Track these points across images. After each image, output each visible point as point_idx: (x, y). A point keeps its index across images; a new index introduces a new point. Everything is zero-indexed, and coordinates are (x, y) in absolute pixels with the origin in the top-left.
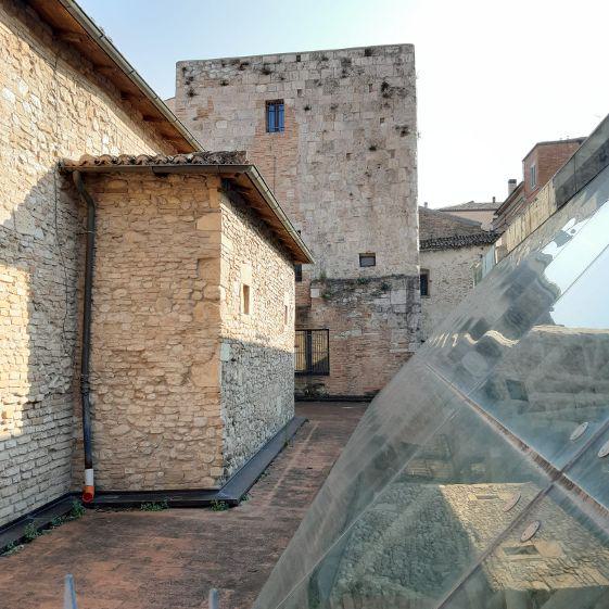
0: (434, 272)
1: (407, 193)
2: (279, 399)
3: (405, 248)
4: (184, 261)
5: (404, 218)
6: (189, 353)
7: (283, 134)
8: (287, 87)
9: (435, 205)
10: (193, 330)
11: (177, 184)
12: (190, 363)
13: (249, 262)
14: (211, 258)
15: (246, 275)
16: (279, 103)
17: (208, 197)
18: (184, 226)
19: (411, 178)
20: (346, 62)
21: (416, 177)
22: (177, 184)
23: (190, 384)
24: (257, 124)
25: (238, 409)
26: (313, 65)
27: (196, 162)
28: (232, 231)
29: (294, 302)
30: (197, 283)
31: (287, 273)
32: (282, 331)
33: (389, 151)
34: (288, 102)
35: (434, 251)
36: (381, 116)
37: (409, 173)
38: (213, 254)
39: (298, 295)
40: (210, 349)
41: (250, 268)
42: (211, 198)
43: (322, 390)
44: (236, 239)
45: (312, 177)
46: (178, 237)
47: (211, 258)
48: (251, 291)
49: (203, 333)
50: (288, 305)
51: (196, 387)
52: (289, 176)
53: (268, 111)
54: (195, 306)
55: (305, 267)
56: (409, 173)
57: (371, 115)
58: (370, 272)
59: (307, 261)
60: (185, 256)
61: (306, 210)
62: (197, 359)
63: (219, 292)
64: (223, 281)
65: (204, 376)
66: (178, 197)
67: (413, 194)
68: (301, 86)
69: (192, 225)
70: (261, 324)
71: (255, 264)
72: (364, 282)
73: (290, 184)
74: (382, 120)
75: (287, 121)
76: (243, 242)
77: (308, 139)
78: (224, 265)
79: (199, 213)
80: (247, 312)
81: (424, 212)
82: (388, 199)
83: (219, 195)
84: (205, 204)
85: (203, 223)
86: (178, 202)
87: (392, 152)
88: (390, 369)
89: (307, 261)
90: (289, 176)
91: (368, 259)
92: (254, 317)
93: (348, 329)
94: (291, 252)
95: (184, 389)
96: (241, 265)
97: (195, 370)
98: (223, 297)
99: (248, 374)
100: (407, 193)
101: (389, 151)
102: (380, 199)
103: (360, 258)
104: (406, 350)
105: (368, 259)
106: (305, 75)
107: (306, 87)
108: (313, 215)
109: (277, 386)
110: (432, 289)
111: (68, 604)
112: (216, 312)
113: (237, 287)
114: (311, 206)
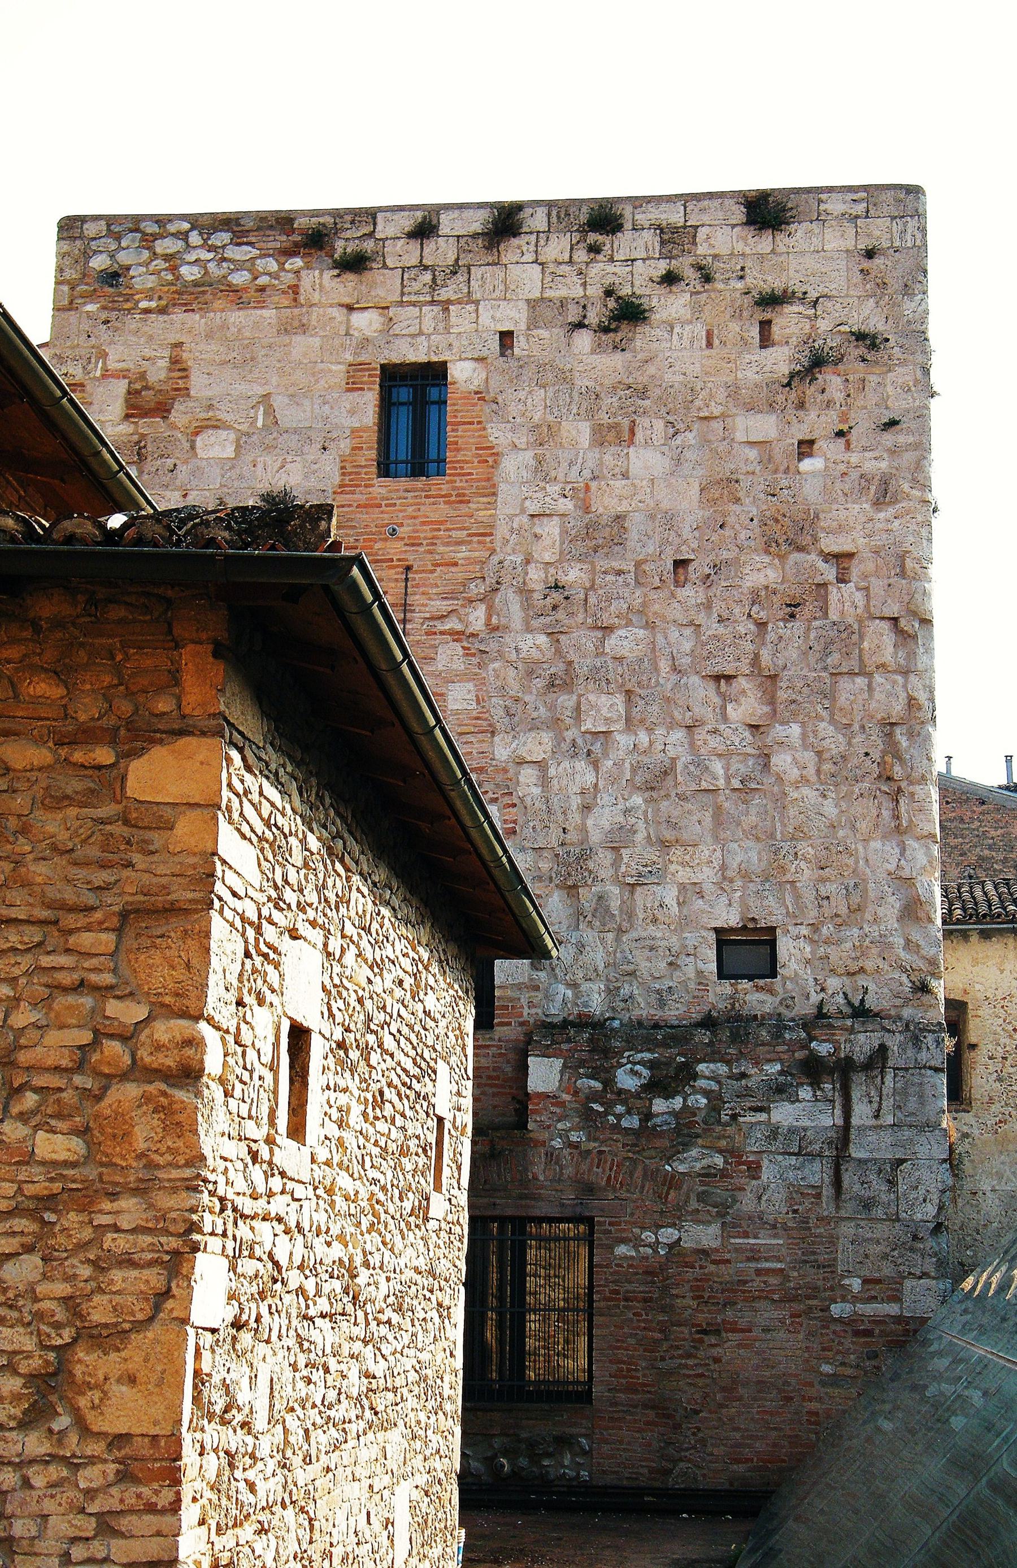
0: (985, 1011)
1: (898, 708)
2: (405, 1493)
3: (891, 909)
4: (70, 921)
5: (887, 804)
6: (62, 1289)
7: (439, 484)
8: (460, 318)
9: (986, 772)
10: (85, 1200)
11: (58, 624)
12: (67, 1335)
13: (316, 936)
14: (172, 910)
15: (302, 985)
16: (433, 375)
17: (175, 678)
18: (74, 785)
19: (912, 655)
20: (674, 238)
21: (929, 651)
22: (58, 624)
23: (62, 1422)
24: (345, 445)
25: (247, 1532)
26: (557, 247)
27: (139, 541)
28: (255, 833)
29: (467, 1103)
30: (113, 1008)
31: (444, 1003)
32: (422, 1211)
33: (829, 557)
34: (462, 373)
35: (986, 935)
36: (800, 432)
37: (904, 637)
38: (183, 895)
39: (484, 1080)
40: (154, 1278)
41: (317, 957)
42: (188, 679)
43: (566, 1466)
44: (271, 846)
45: (542, 639)
46: (52, 825)
47: (172, 910)
48: (318, 1048)
49: (130, 1210)
50: (448, 1116)
51: (85, 1430)
52: (457, 635)
53: (387, 406)
54: (99, 1098)
55: (508, 971)
56: (904, 637)
57: (764, 426)
58: (755, 999)
59: (531, 948)
60: (69, 895)
61: (521, 762)
62: (96, 1317)
63: (196, 1043)
64: (217, 998)
65: (119, 1391)
66: (59, 673)
67: (916, 716)
68: (513, 316)
69: (109, 781)
70: (344, 1181)
71: (335, 944)
72: (730, 1029)
73: (459, 665)
74: (806, 447)
75: (460, 441)
76: (297, 858)
77: (532, 507)
78: (225, 942)
79: (138, 736)
80: (297, 1131)
81: (958, 796)
82: (825, 728)
83: (217, 670)
84: (164, 705)
85: (155, 776)
86: (61, 691)
87: (841, 559)
88: (834, 1381)
89: (531, 948)
90: (457, 635)
91: (747, 951)
92: (323, 1155)
93: (675, 1217)
94: (464, 897)
95: (35, 1444)
96: (286, 944)
97: (87, 1361)
98: (213, 1062)
99: (291, 1389)
100: (898, 708)
101: (829, 557)
102: (795, 729)
103: (721, 944)
104: (893, 1309)
105: (747, 951)
106: (528, 280)
107: (533, 324)
108: (545, 781)
109: (395, 1437)
110: (981, 1079)
111: (192, 1544)
112: (181, 1126)
113: (264, 1027)
114: (537, 745)
